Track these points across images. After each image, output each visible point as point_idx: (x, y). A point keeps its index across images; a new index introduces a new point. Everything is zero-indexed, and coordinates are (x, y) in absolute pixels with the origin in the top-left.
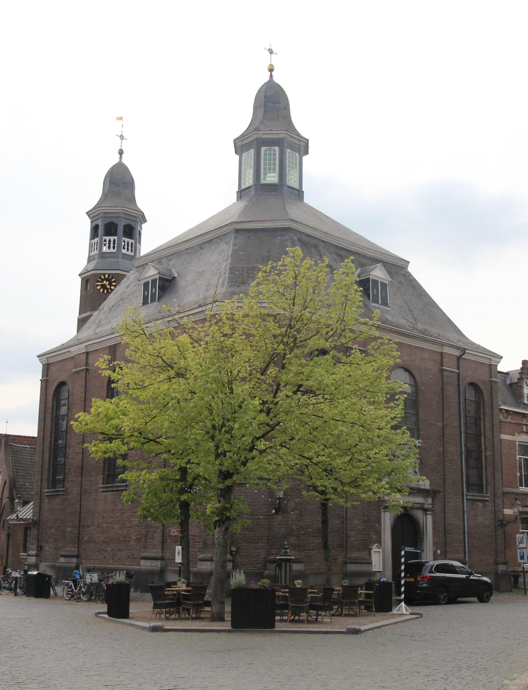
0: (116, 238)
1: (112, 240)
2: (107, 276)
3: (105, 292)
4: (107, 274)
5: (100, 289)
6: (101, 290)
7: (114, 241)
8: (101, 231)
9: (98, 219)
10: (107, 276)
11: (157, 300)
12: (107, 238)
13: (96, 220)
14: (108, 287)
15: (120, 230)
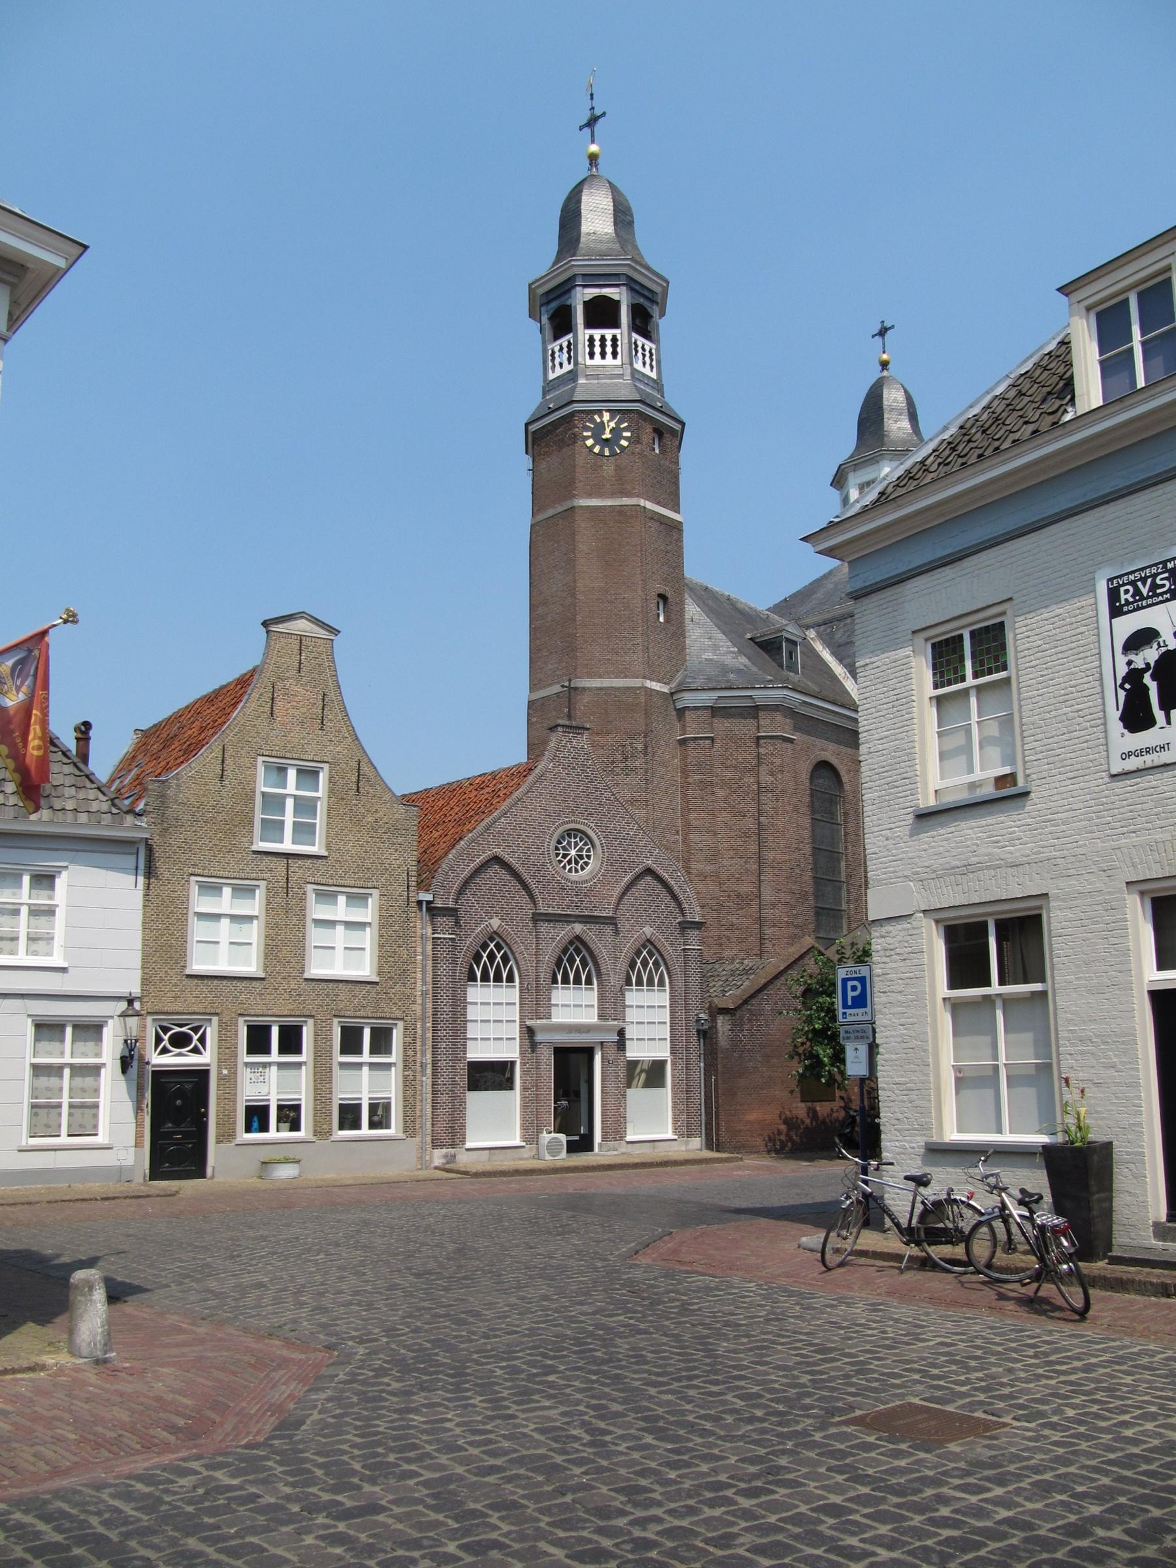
1: (609, 337)
7: (614, 339)
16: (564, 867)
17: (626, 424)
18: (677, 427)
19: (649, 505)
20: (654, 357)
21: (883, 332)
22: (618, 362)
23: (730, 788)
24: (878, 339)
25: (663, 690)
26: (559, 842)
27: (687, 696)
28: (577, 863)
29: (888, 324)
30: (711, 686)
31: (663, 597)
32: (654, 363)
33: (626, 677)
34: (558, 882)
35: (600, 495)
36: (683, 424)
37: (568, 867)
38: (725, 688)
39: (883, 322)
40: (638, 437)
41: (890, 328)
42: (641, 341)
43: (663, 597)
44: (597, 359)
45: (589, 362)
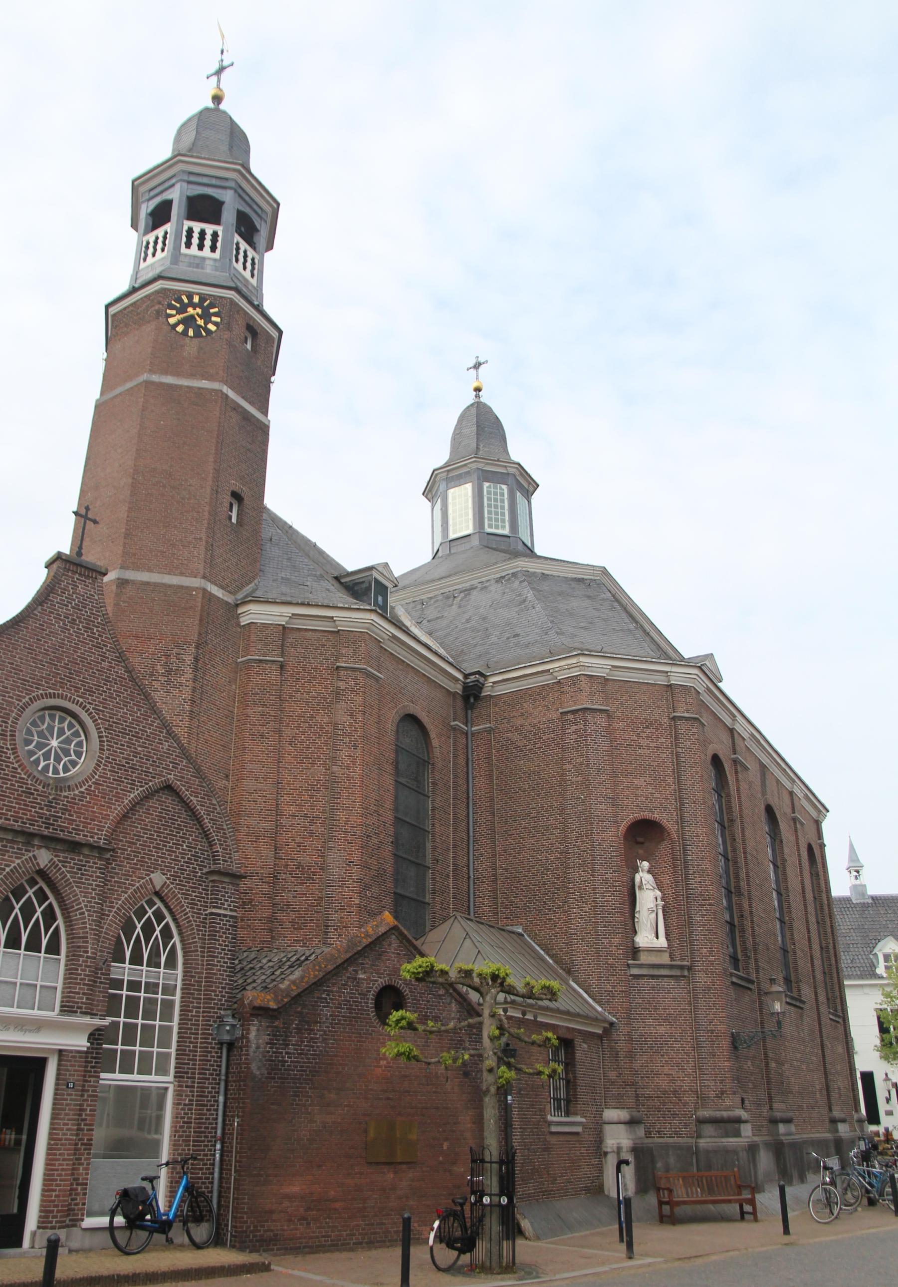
0: (219, 229)
2: (196, 299)
3: (191, 333)
7: (215, 235)
9: (173, 185)
10: (196, 299)
12: (197, 227)
13: (162, 192)
14: (201, 322)
15: (229, 215)
16: (37, 762)
17: (216, 310)
18: (275, 334)
19: (231, 394)
20: (256, 266)
21: (477, 366)
22: (217, 255)
23: (298, 727)
24: (473, 371)
25: (226, 599)
26: (34, 724)
27: (253, 607)
28: (58, 759)
29: (481, 360)
30: (284, 599)
31: (236, 496)
32: (256, 272)
33: (182, 574)
34: (22, 781)
35: (178, 374)
36: (280, 333)
37: (42, 764)
38: (303, 604)
39: (478, 357)
40: (229, 324)
41: (484, 363)
42: (243, 245)
43: (236, 496)
44: (194, 250)
45: (184, 250)
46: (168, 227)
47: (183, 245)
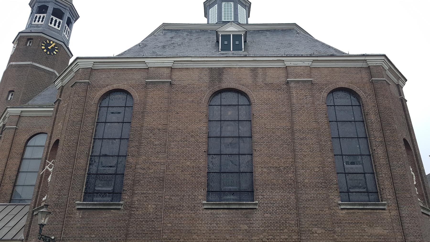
4: (52, 41)
5: (44, 49)
6: (45, 51)
7: (60, 22)
8: (50, 10)
11: (243, 50)
12: (55, 18)
45: (49, 24)
46: (45, 15)
47: (49, 23)
